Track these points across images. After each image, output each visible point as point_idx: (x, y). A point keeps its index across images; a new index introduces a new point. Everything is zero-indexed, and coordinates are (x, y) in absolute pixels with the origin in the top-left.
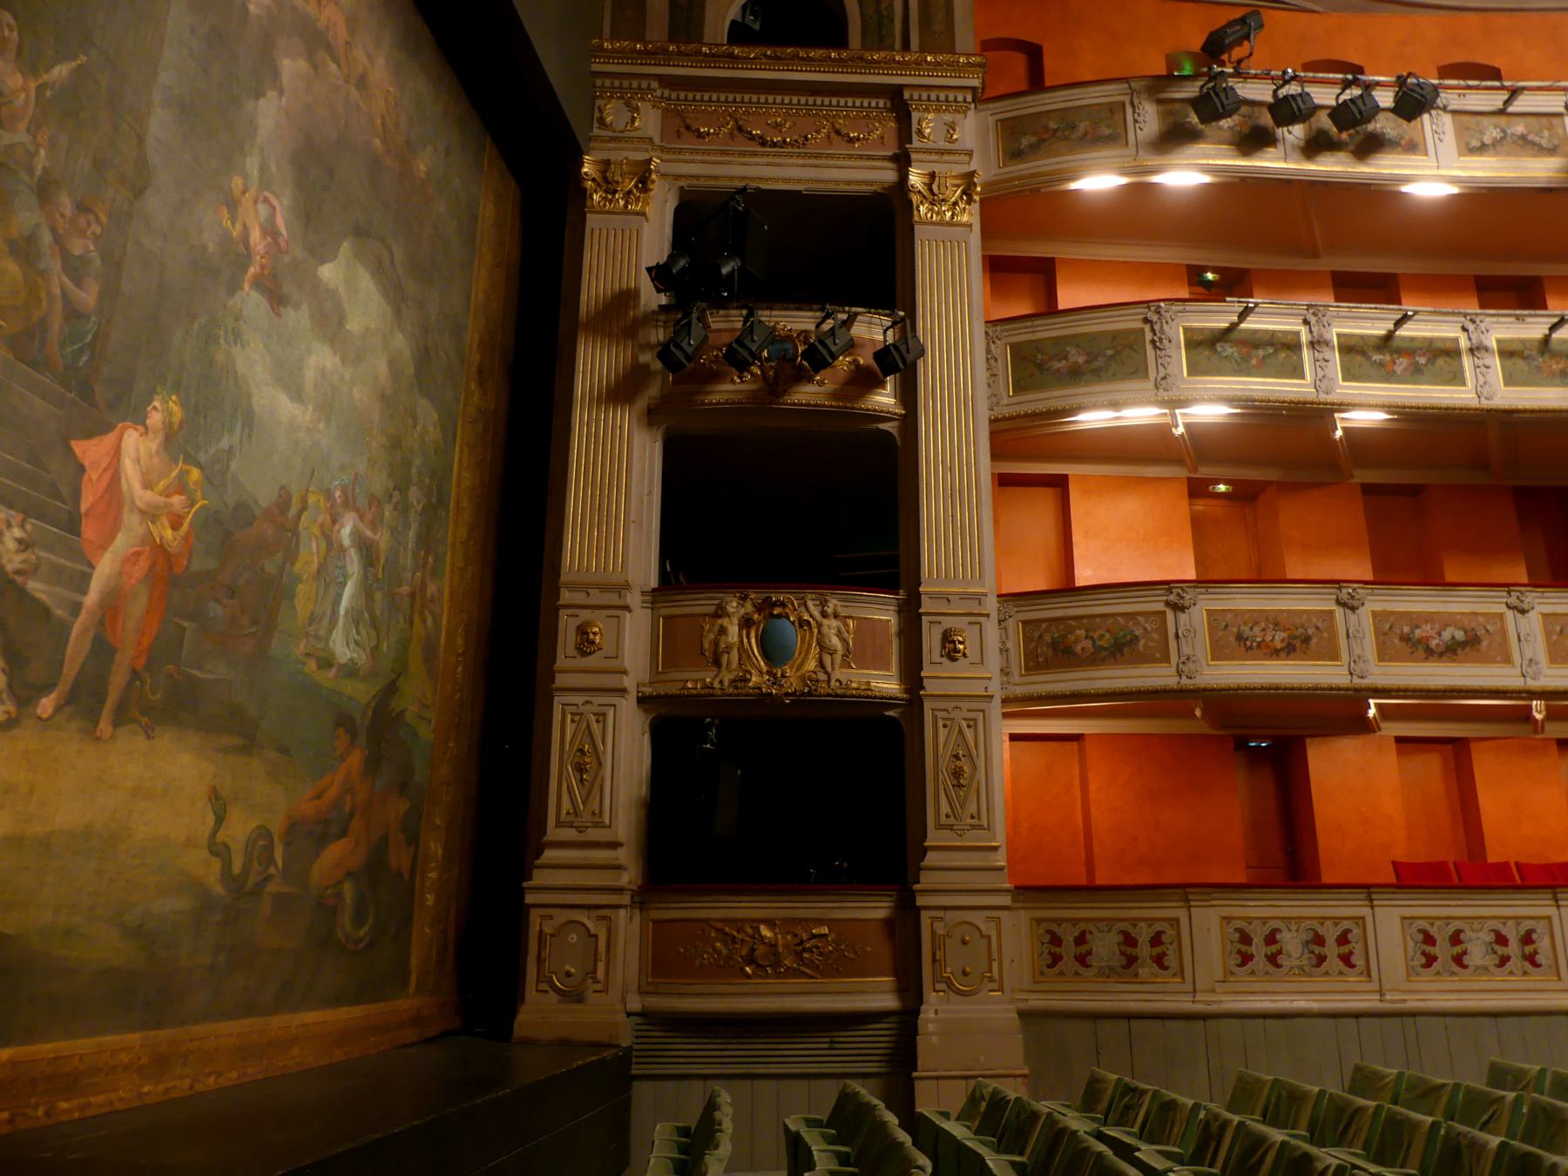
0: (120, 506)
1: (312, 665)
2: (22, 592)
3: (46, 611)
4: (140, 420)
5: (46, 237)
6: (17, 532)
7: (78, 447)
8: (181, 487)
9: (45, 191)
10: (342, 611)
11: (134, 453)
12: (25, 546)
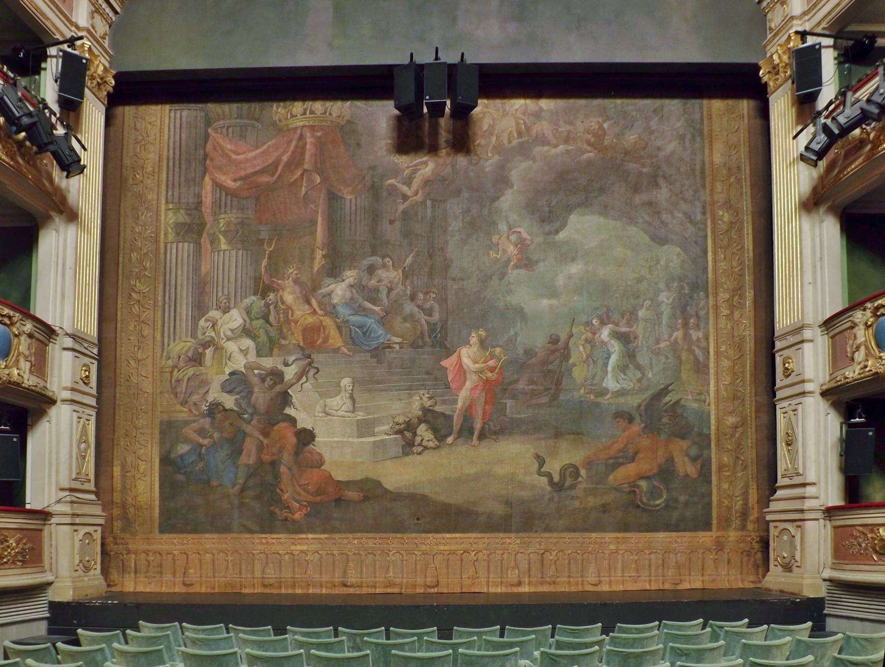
0: (465, 373)
1: (592, 397)
2: (434, 412)
3: (443, 414)
4: (467, 343)
5: (417, 309)
6: (427, 396)
7: (444, 363)
8: (492, 356)
9: (413, 298)
10: (609, 369)
11: (468, 356)
12: (430, 398)
